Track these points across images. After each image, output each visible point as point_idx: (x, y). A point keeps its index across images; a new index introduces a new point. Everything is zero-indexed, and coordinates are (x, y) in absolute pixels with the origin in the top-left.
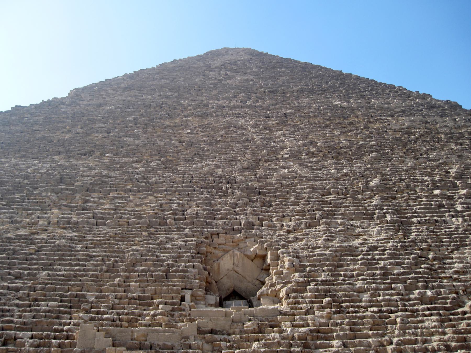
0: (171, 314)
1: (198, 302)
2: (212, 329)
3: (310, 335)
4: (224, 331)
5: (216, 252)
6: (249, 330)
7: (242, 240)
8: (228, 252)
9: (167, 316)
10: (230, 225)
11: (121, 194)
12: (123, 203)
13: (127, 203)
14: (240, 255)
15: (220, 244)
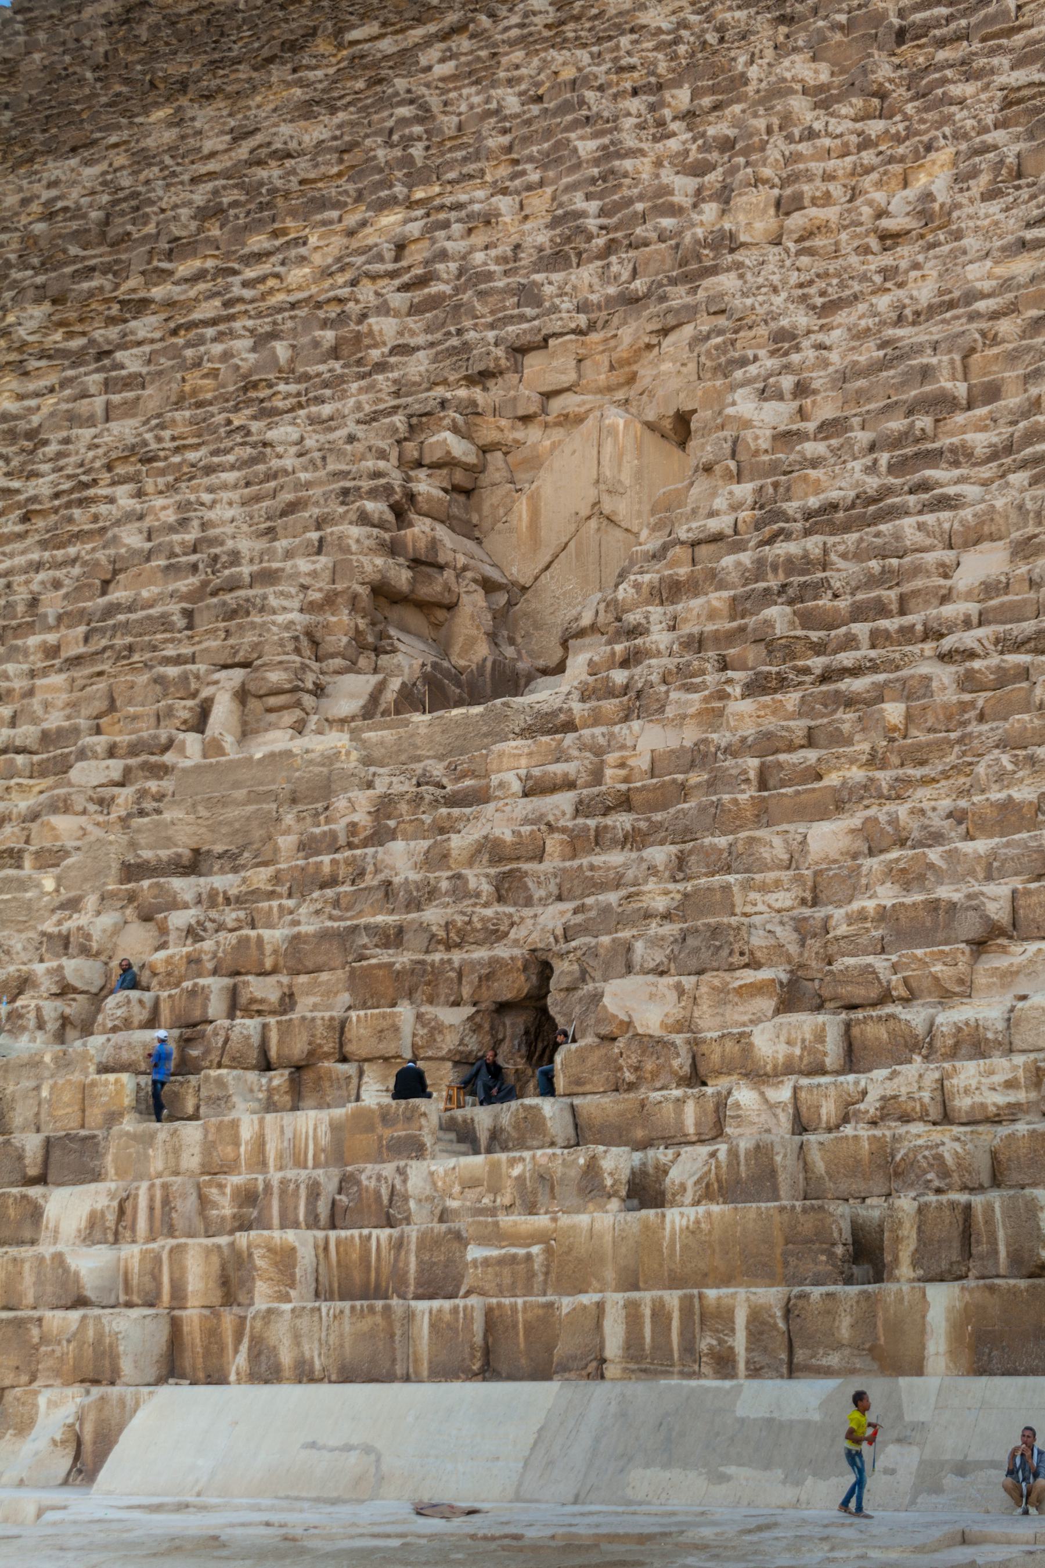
0: (101, 802)
1: (272, 717)
2: (196, 852)
3: (564, 830)
4: (246, 855)
5: (532, 434)
6: (325, 833)
7: (649, 347)
8: (579, 419)
9: (84, 812)
10: (625, 275)
11: (284, 232)
12: (262, 279)
13: (277, 276)
14: (626, 425)
15: (557, 393)
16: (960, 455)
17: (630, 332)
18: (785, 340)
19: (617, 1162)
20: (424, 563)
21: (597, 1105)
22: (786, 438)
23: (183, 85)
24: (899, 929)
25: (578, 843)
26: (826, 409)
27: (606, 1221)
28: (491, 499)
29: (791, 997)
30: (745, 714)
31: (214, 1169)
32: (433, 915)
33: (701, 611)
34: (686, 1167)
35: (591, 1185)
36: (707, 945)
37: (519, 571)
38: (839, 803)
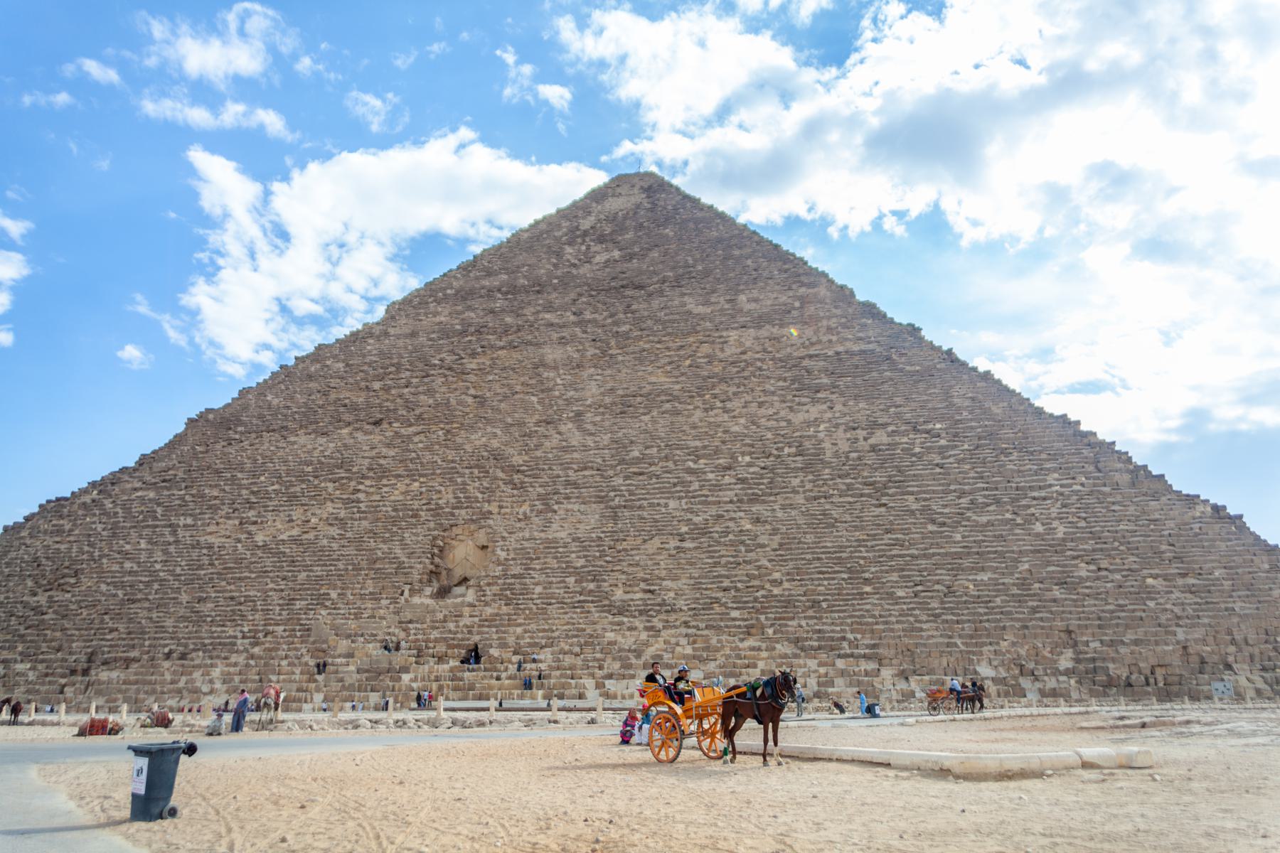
16: (534, 569)
17: (473, 527)
18: (504, 539)
19: (495, 674)
20: (437, 566)
21: (488, 666)
22: (506, 560)
23: (349, 424)
24: (530, 645)
25: (480, 626)
26: (512, 556)
27: (494, 682)
28: (446, 552)
29: (515, 653)
30: (505, 609)
31: (430, 672)
32: (459, 636)
33: (495, 589)
34: (504, 675)
35: (492, 677)
36: (503, 645)
37: (450, 566)
38: (520, 625)
